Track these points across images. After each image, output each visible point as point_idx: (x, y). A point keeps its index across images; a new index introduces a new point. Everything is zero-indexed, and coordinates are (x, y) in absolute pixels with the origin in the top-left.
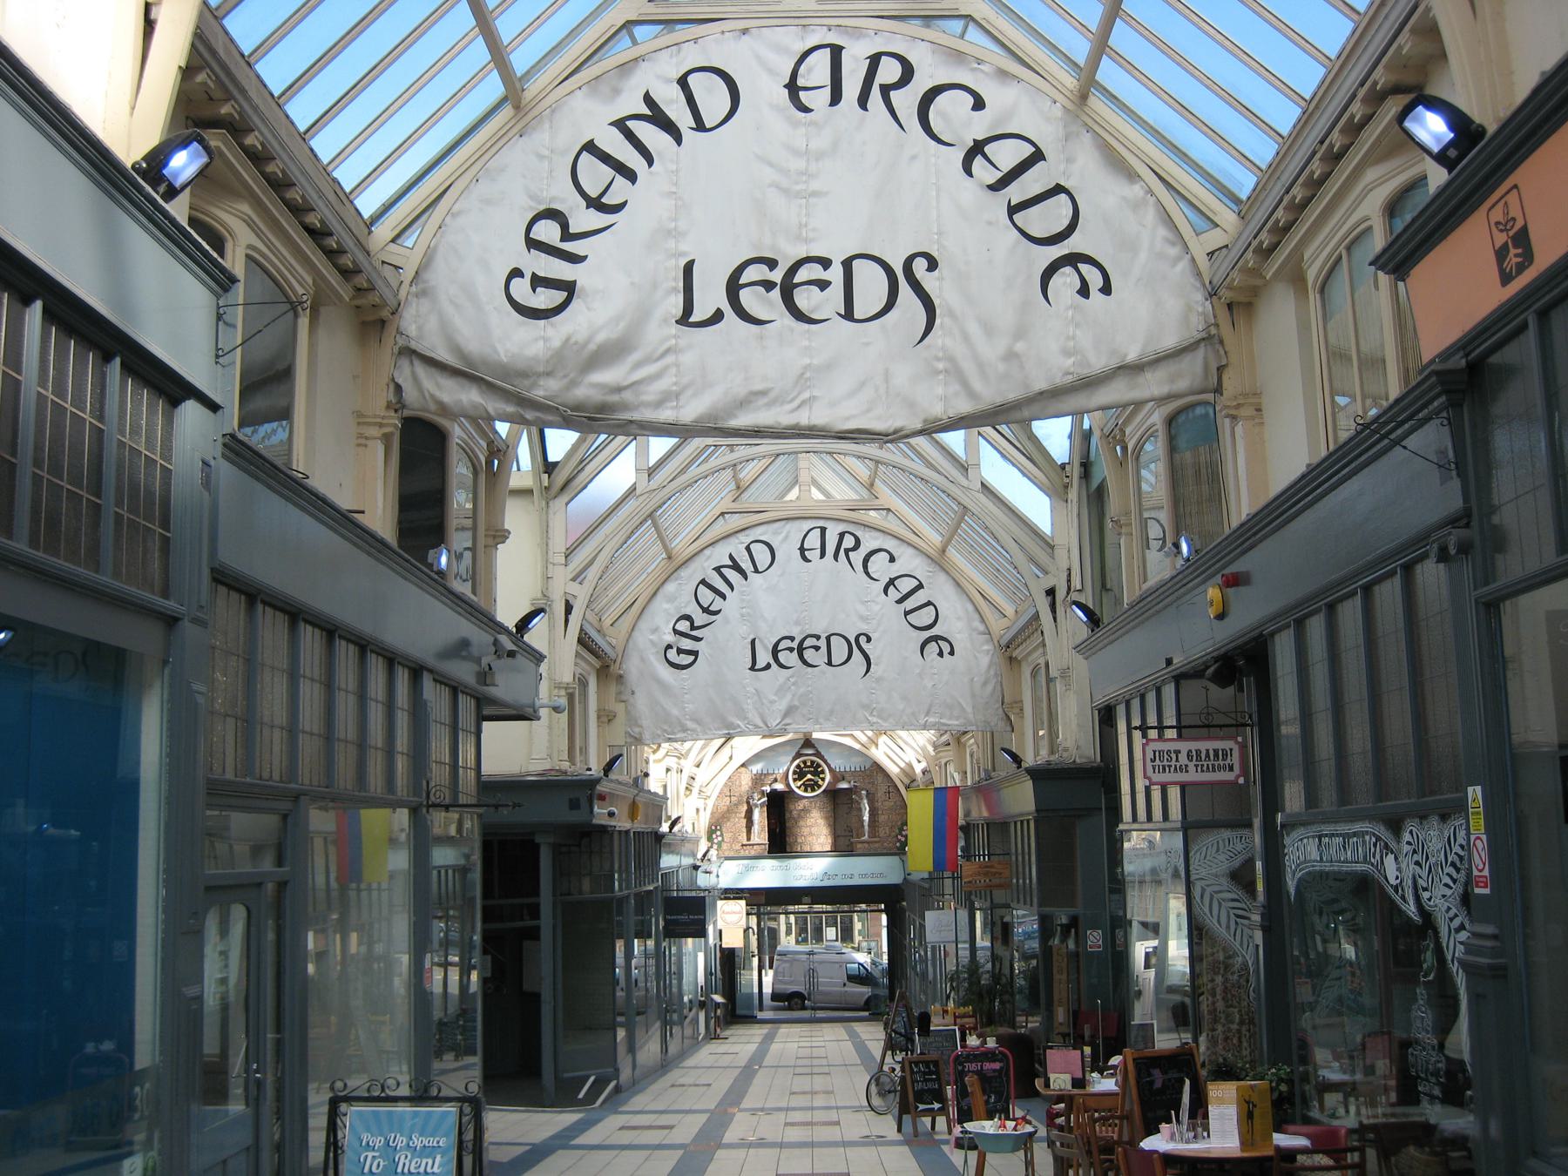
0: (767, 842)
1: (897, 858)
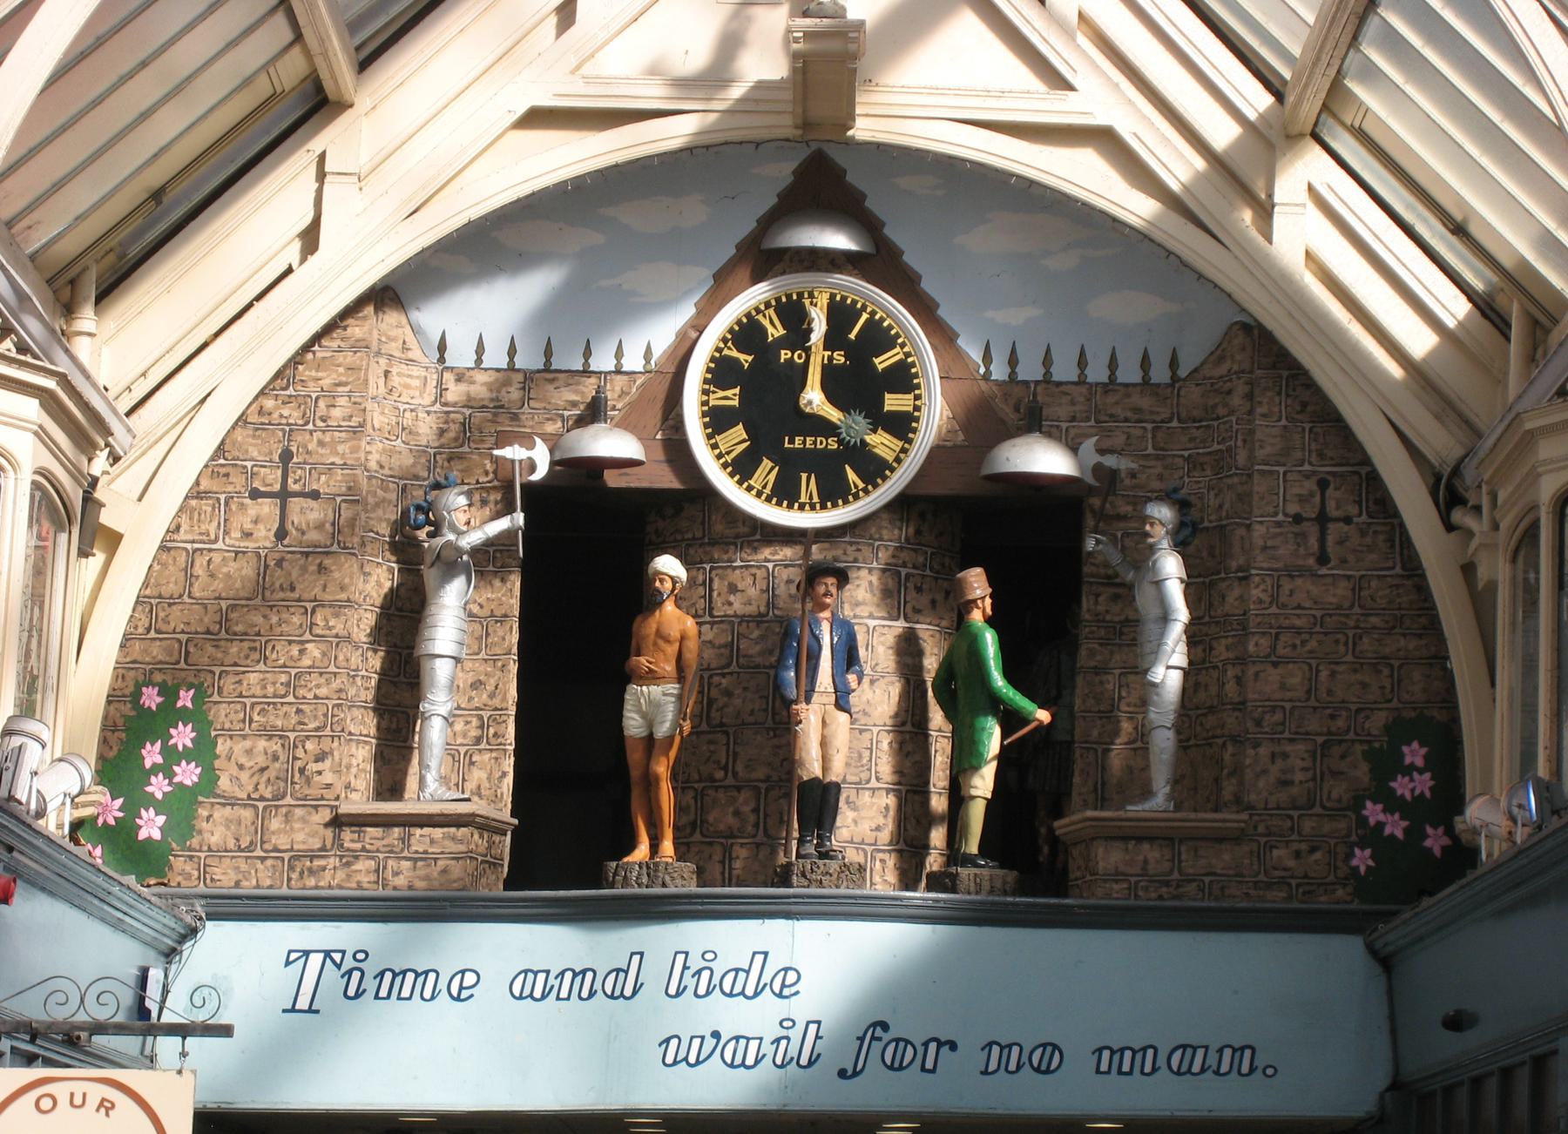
0: (503, 812)
1: (1347, 951)
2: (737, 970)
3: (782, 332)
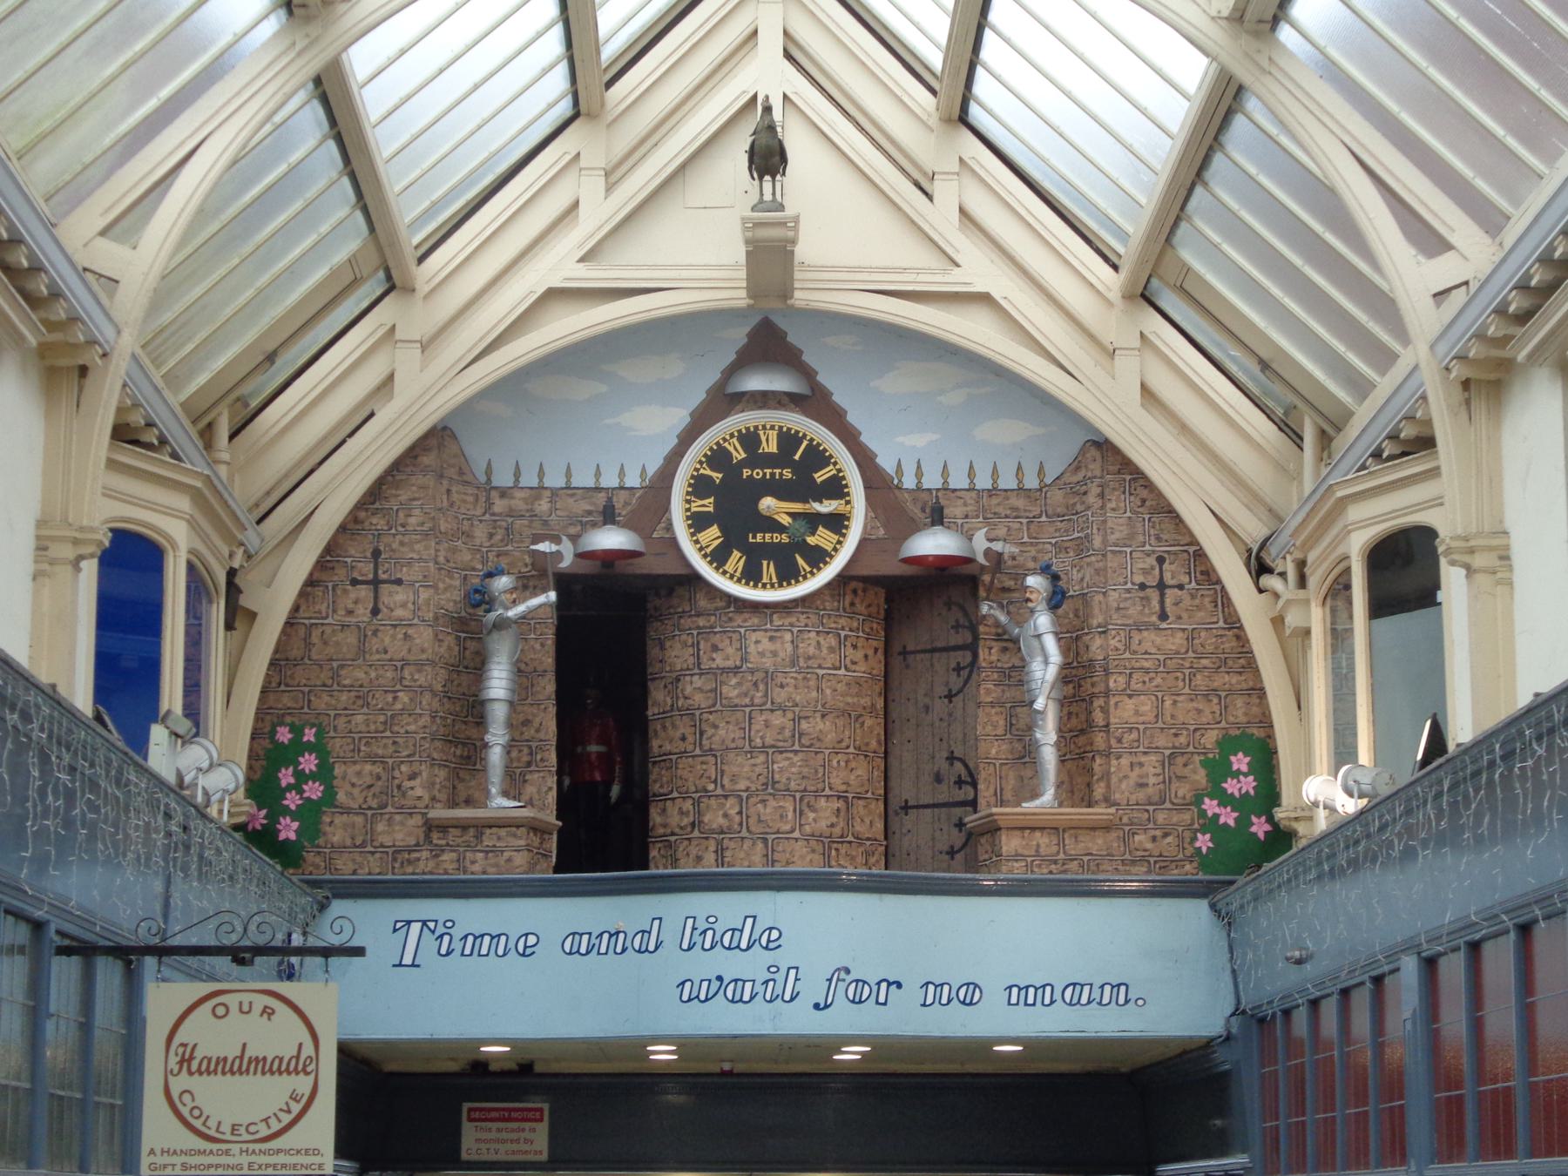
0: (550, 817)
1: (1196, 911)
2: (734, 930)
3: (744, 455)
